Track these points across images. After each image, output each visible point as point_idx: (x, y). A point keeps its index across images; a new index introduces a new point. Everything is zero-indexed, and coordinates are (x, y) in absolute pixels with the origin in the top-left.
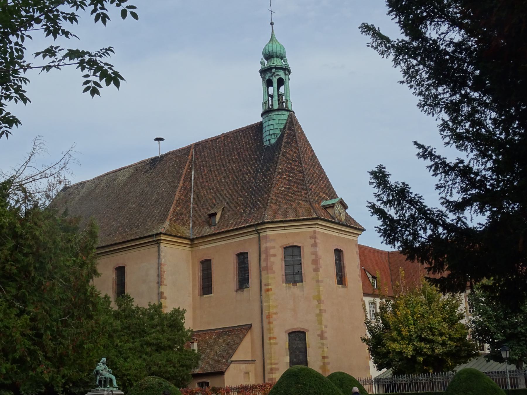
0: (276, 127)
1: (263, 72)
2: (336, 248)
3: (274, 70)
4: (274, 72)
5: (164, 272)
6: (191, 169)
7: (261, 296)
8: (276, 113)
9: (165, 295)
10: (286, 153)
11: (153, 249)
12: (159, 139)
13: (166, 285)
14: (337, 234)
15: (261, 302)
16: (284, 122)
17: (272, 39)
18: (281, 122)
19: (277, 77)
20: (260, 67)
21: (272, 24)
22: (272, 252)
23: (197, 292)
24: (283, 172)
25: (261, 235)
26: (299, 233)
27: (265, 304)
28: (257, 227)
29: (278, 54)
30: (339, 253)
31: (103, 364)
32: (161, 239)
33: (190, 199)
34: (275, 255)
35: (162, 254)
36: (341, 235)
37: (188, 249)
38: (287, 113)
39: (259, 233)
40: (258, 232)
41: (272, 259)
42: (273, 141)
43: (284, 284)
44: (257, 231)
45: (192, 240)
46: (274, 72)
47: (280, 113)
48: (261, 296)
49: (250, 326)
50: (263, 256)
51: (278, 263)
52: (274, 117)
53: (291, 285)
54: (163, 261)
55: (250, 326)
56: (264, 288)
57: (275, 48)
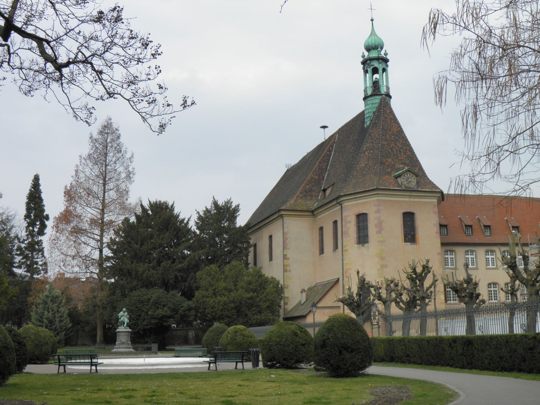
0: (370, 110)
1: (364, 63)
2: (406, 211)
3: (368, 62)
4: (375, 61)
5: (287, 239)
6: (330, 151)
7: (343, 255)
8: (370, 99)
9: (288, 256)
10: (372, 133)
11: (279, 223)
12: (324, 127)
13: (289, 249)
14: (407, 199)
15: (343, 261)
16: (376, 105)
17: (373, 33)
18: (374, 105)
19: (372, 67)
20: (362, 59)
21: (372, 20)
22: (348, 219)
23: (318, 252)
24: (366, 150)
25: (343, 205)
26: (366, 202)
27: (344, 262)
28: (337, 200)
29: (374, 46)
30: (335, 222)
31: (124, 312)
32: (282, 214)
33: (324, 177)
34: (350, 222)
35: (285, 225)
36: (411, 200)
37: (312, 219)
38: (379, 97)
39: (341, 205)
40: (340, 204)
41: (348, 225)
42: (368, 123)
43: (356, 245)
44: (338, 203)
45: (312, 212)
46: (375, 61)
47: (373, 98)
48: (343, 255)
49: (338, 280)
50: (343, 223)
51: (351, 228)
52: (369, 102)
53: (361, 245)
54: (286, 230)
55: (338, 280)
56: (344, 249)
57: (373, 41)
